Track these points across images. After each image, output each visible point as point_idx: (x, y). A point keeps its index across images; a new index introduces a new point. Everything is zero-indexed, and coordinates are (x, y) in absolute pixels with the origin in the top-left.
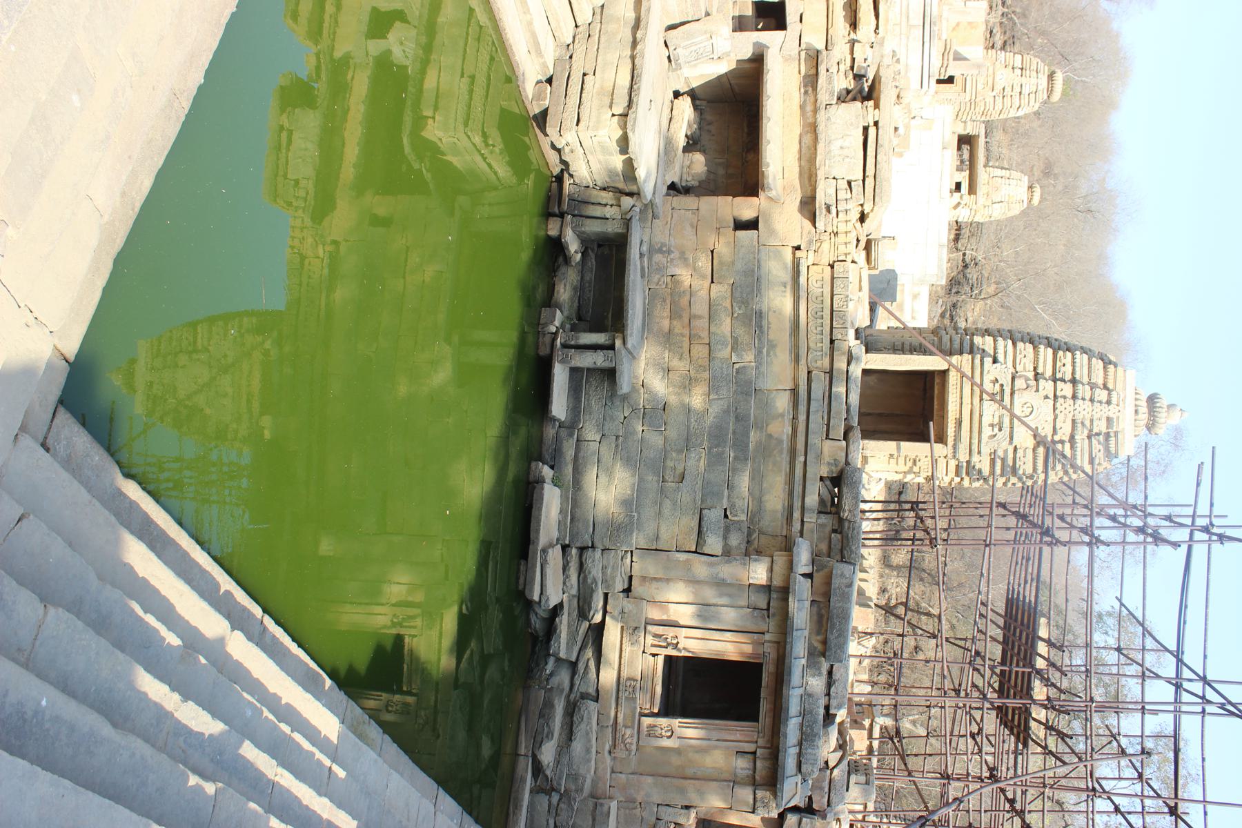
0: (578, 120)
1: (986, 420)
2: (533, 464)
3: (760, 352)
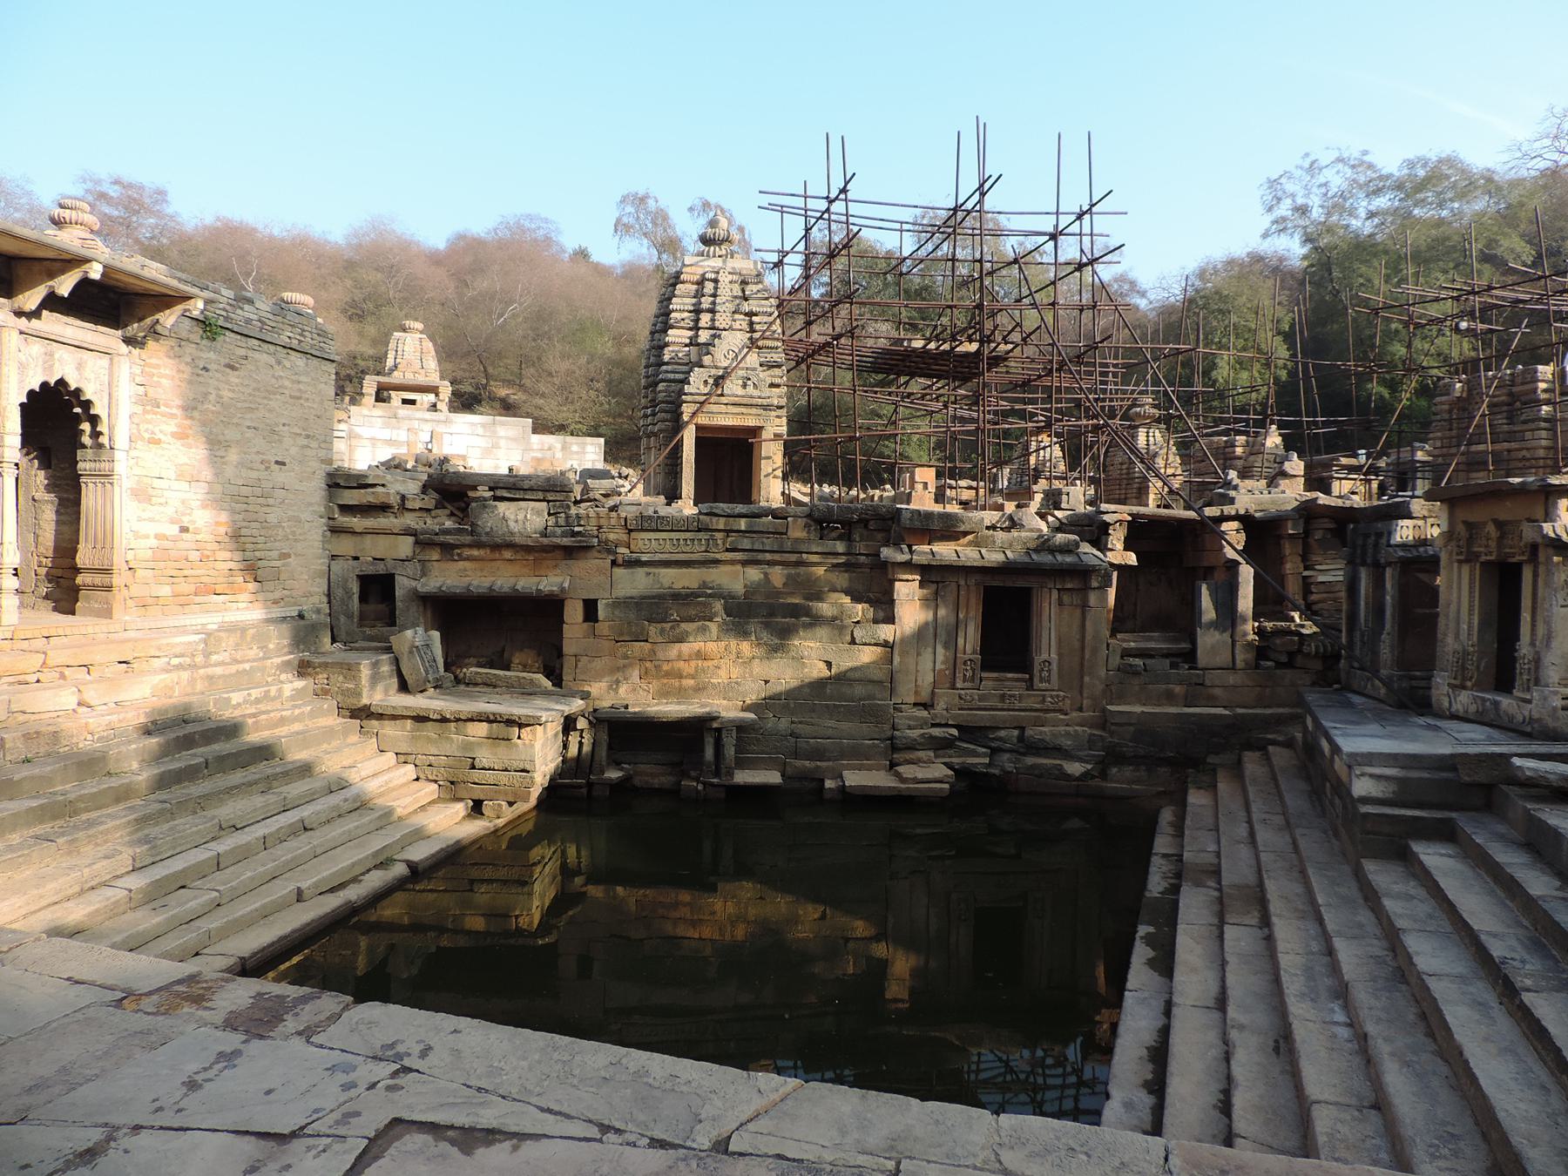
0: (523, 771)
1: (740, 391)
2: (827, 796)
3: (710, 596)
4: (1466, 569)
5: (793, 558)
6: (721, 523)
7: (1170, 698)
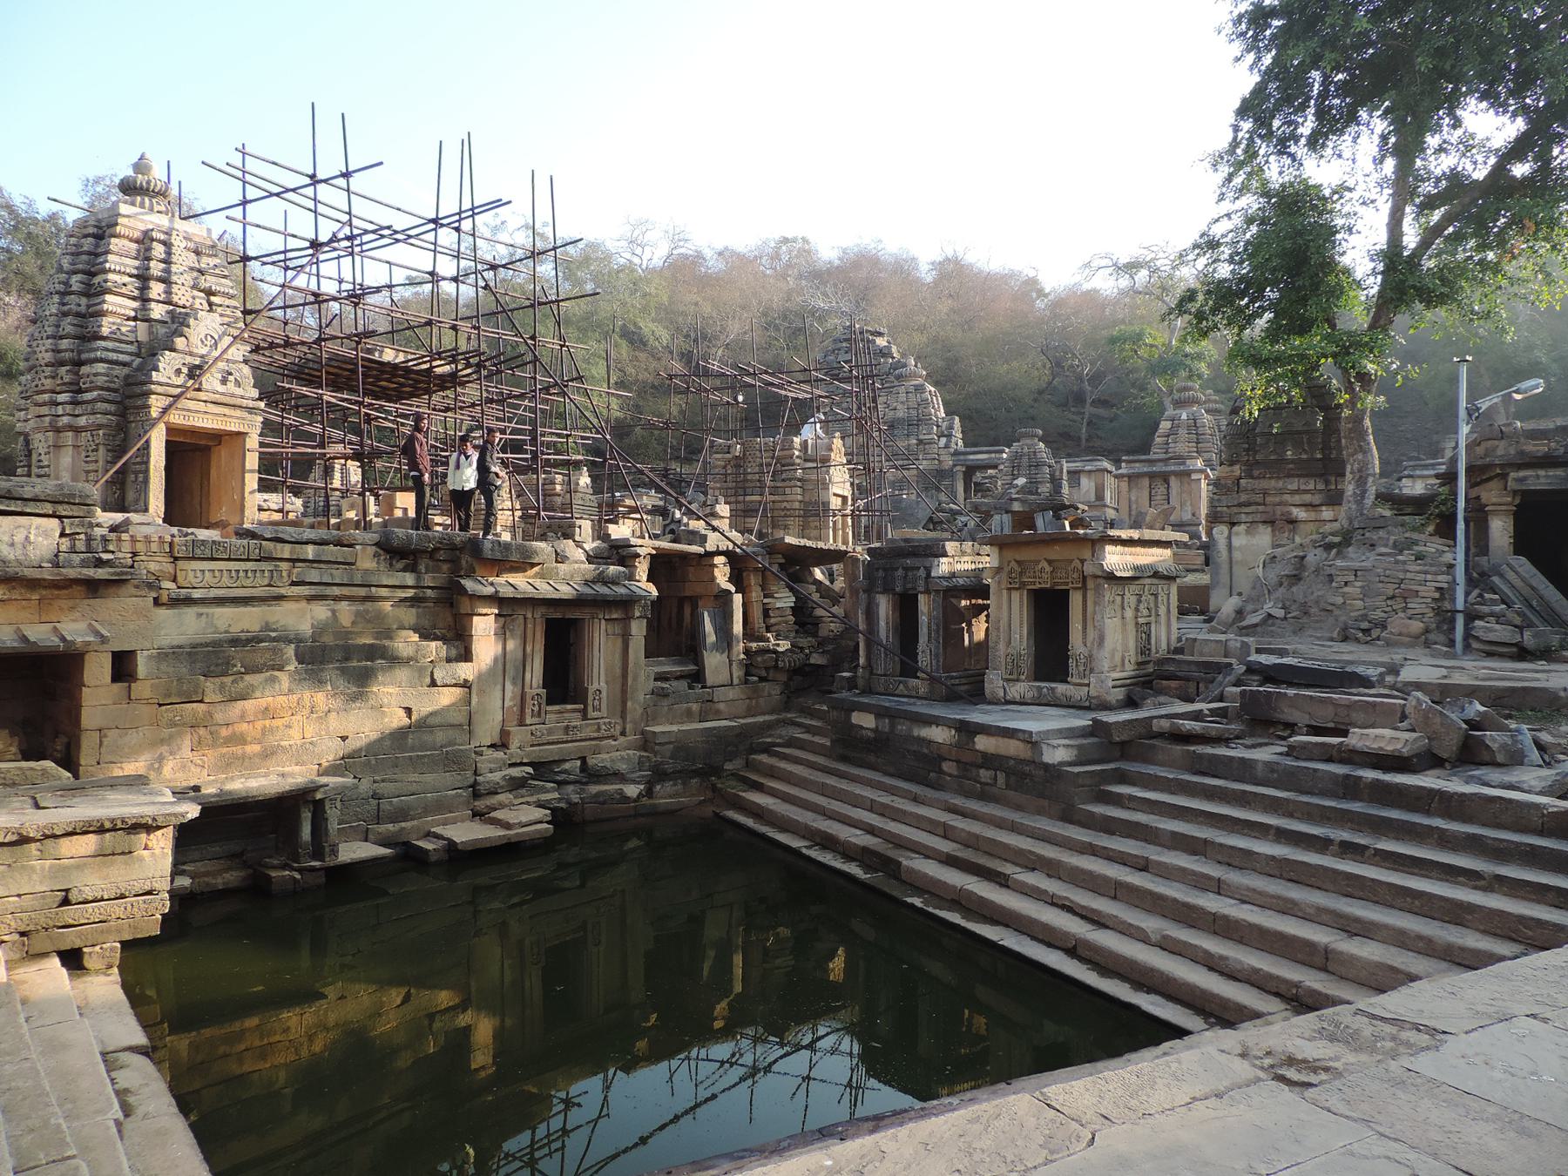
0: (149, 893)
1: (221, 388)
2: (433, 858)
3: (274, 640)
4: (1015, 595)
5: (362, 592)
6: (285, 551)
7: (689, 715)
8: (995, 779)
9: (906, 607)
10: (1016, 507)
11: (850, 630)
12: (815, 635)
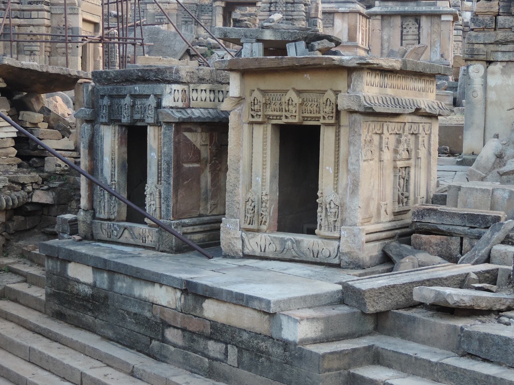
4: (258, 130)
8: (226, 354)
9: (135, 138)
10: (268, 35)
11: (73, 170)
12: (40, 169)
